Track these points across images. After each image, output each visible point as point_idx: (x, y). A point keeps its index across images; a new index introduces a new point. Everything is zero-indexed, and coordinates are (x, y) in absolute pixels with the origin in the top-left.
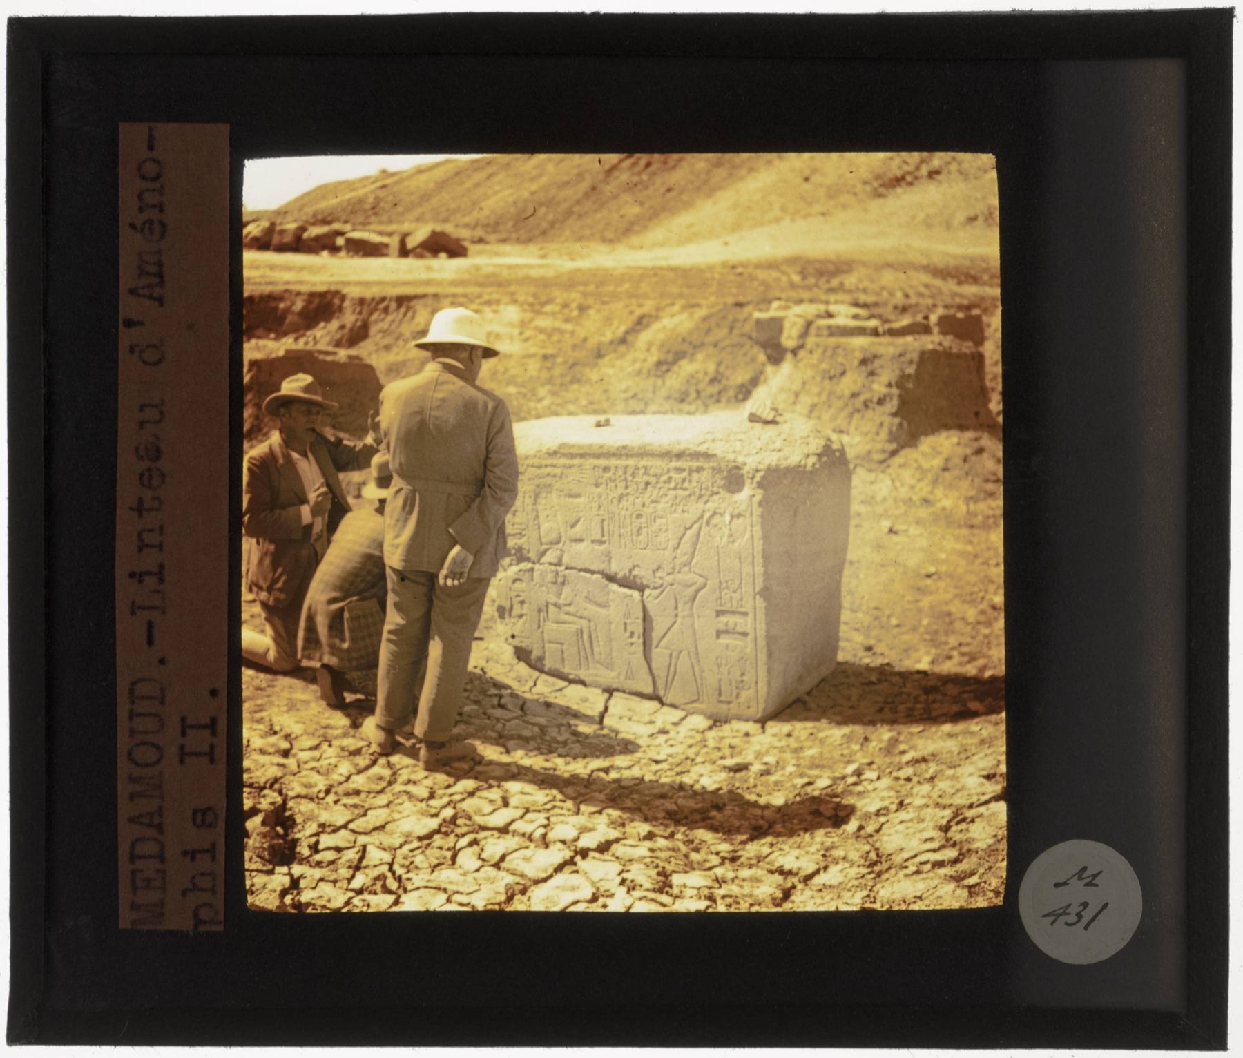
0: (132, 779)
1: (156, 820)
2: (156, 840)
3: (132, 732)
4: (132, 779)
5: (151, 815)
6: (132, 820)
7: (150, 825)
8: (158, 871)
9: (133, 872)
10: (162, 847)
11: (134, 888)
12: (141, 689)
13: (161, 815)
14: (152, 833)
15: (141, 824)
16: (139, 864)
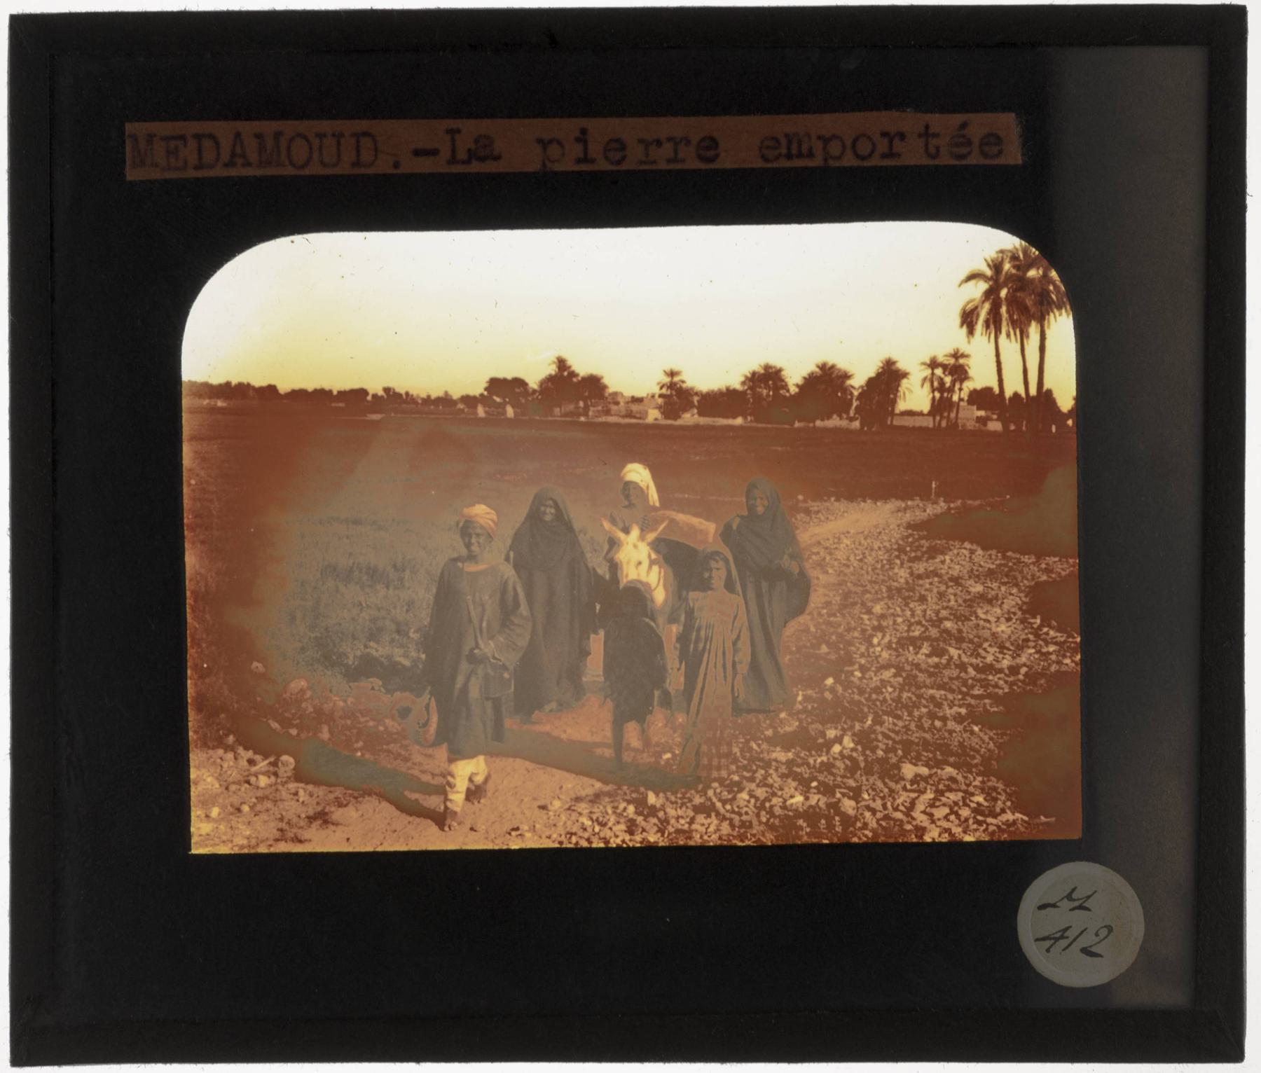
0: (278, 135)
1: (240, 161)
2: (218, 159)
3: (321, 136)
4: (278, 135)
5: (244, 156)
6: (238, 135)
7: (233, 155)
8: (186, 162)
9: (182, 138)
10: (212, 167)
11: (167, 139)
12: (365, 141)
13: (244, 165)
14: (225, 156)
15: (234, 145)
16: (192, 143)
